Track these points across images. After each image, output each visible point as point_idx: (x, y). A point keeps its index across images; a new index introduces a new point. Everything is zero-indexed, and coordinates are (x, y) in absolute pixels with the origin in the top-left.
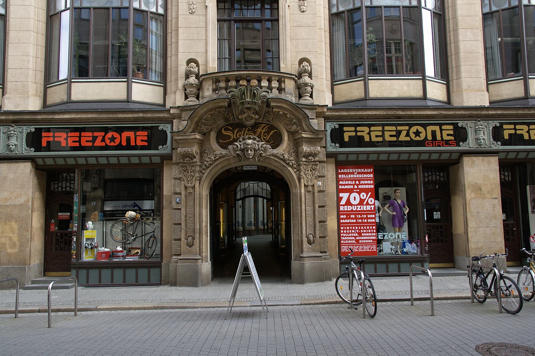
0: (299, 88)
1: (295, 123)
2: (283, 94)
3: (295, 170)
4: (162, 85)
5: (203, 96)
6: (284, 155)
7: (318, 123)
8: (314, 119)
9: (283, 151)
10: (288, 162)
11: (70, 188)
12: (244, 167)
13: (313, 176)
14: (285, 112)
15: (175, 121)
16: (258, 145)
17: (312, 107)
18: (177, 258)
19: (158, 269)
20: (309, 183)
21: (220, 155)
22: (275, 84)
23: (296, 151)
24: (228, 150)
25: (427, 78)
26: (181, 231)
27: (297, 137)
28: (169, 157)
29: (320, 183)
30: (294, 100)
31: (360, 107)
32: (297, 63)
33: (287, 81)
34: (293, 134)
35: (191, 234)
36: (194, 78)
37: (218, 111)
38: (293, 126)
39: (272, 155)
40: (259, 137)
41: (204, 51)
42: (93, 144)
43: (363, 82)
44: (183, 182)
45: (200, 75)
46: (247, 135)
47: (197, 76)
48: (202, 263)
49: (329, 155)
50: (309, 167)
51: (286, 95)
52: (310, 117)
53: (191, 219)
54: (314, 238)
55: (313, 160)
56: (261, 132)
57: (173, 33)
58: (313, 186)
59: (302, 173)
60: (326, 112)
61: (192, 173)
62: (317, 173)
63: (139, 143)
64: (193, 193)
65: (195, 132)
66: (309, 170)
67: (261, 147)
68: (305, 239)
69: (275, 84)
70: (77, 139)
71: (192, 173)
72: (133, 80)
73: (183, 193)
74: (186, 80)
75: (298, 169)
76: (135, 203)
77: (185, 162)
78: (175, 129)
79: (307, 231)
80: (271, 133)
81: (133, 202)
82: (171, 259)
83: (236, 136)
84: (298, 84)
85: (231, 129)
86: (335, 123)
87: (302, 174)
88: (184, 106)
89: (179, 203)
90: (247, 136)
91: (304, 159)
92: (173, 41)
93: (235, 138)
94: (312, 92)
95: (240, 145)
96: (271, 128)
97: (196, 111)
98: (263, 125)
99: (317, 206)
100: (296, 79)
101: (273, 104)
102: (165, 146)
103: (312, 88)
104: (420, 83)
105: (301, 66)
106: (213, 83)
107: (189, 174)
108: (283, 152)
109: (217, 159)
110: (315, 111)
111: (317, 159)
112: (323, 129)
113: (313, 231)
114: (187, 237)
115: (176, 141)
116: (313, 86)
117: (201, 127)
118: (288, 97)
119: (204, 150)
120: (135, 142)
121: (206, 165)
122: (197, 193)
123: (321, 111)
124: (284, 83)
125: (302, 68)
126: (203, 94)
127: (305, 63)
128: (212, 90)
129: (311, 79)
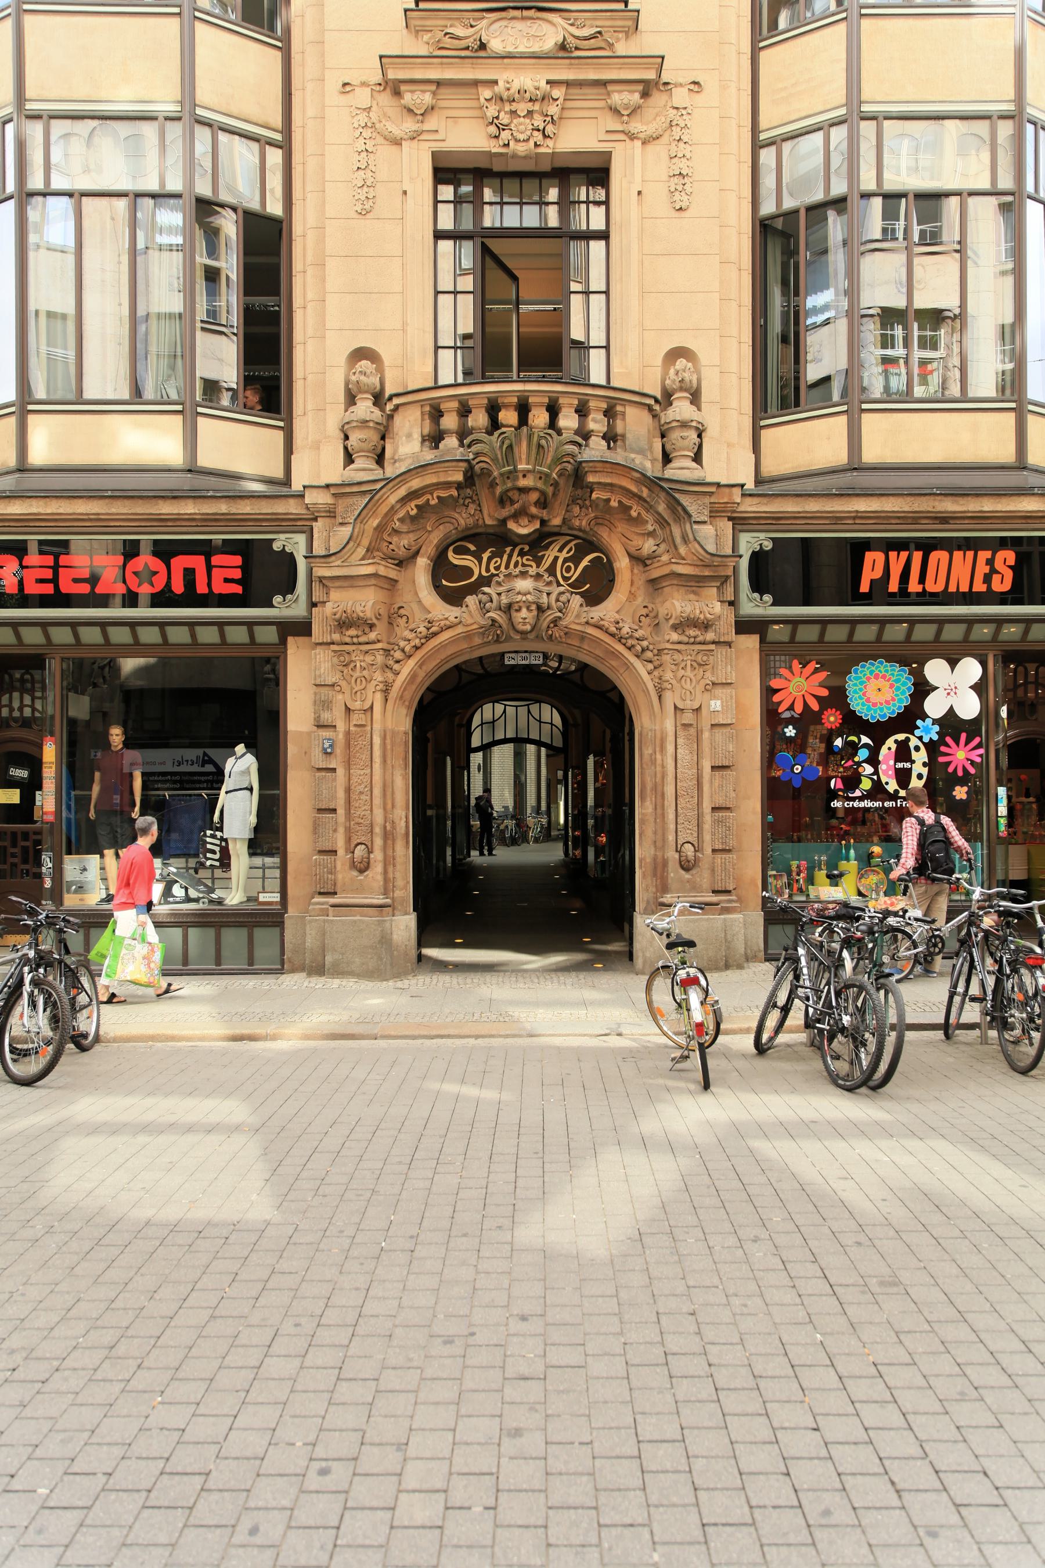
0: (663, 436)
1: (651, 534)
2: (619, 450)
3: (650, 666)
4: (281, 424)
5: (396, 457)
6: (621, 625)
8: (704, 522)
9: (617, 612)
10: (630, 642)
11: (34, 710)
12: (506, 655)
14: (627, 502)
15: (318, 526)
16: (548, 594)
17: (700, 488)
19: (277, 930)
20: (688, 702)
21: (442, 623)
22: (596, 423)
24: (464, 609)
25: (1031, 407)
26: (335, 831)
27: (655, 574)
28: (302, 628)
29: (719, 703)
30: (650, 467)
31: (834, 491)
32: (659, 361)
33: (631, 412)
34: (647, 565)
35: (362, 839)
36: (370, 403)
37: (439, 497)
39: (587, 623)
41: (399, 327)
42: (93, 587)
43: (843, 419)
44: (340, 697)
45: (387, 395)
46: (516, 565)
47: (378, 398)
49: (744, 626)
51: (626, 454)
52: (696, 517)
53: (363, 797)
56: (556, 558)
57: (310, 271)
58: (698, 710)
59: (668, 675)
61: (365, 673)
62: (708, 674)
63: (220, 588)
64: (369, 728)
65: (374, 557)
67: (557, 600)
68: (672, 855)
69: (596, 423)
70: (49, 574)
71: (365, 673)
72: (200, 410)
73: (341, 727)
74: (346, 411)
75: (657, 663)
76: (205, 754)
77: (348, 640)
78: (318, 549)
80: (585, 562)
81: (200, 752)
82: (310, 904)
83: (488, 570)
84: (662, 422)
85: (472, 548)
86: (762, 535)
87: (668, 678)
88: (342, 485)
89: (330, 753)
90: (517, 570)
91: (675, 636)
92: (310, 295)
93: (484, 574)
94: (700, 446)
95: (499, 594)
96: (587, 545)
97: (377, 497)
98: (563, 540)
100: (657, 407)
101: (591, 478)
102: (289, 596)
103: (700, 436)
104: (1010, 418)
105: (672, 371)
106: (423, 420)
107: (357, 674)
108: (617, 617)
109: (435, 634)
110: (707, 500)
112: (729, 552)
113: (696, 835)
114: (353, 846)
115: (321, 581)
116: (704, 430)
120: (209, 585)
121: (403, 650)
122: (377, 726)
123: (725, 500)
124: (624, 419)
125: (675, 377)
126: (395, 451)
127: (681, 363)
129: (699, 409)
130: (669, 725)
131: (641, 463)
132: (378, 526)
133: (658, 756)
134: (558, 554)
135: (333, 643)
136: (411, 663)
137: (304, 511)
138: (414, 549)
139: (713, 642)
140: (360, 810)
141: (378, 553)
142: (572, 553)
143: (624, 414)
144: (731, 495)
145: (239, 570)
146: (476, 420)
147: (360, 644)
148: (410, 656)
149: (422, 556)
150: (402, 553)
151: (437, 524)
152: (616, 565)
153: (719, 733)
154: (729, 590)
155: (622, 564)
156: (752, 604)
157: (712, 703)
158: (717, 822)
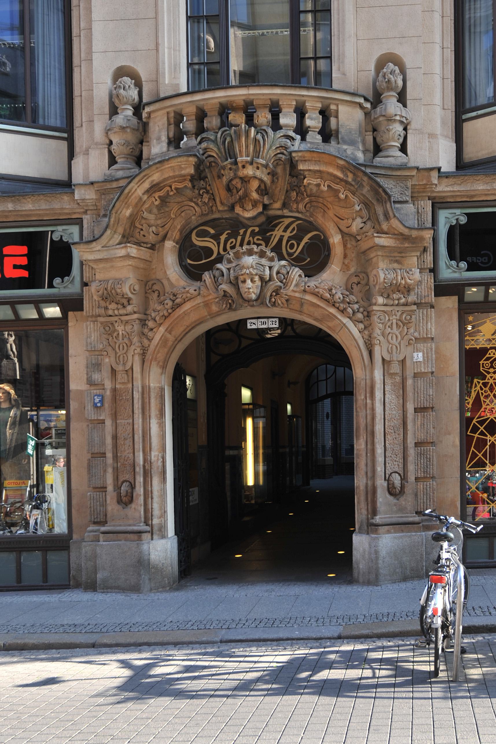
3: (361, 326)
7: (418, 212)
8: (406, 202)
13: (402, 339)
18: (98, 530)
23: (363, 282)
29: (420, 355)
38: (353, 220)
40: (277, 249)
48: (152, 539)
50: (394, 317)
51: (339, 146)
54: (403, 482)
55: (403, 301)
58: (403, 362)
60: (436, 185)
62: (412, 330)
66: (394, 326)
75: (366, 323)
77: (110, 312)
79: (387, 464)
80: (306, 240)
83: (225, 250)
85: (212, 231)
86: (458, 211)
98: (287, 221)
99: (410, 408)
111: (412, 298)
113: (401, 466)
117: (142, 230)
118: (345, 151)
119: (153, 285)
128: (167, 141)
130: (378, 374)
131: (352, 153)
132: (131, 215)
133: (369, 401)
134: (283, 234)
135: (99, 316)
136: (162, 329)
137: (76, 206)
138: (162, 232)
139: (415, 304)
140: (125, 452)
141: (131, 239)
142: (295, 232)
143: (337, 111)
144: (429, 177)
145: (26, 258)
146: (210, 122)
147: (121, 315)
148: (160, 325)
149: (169, 240)
150: (151, 238)
151: (179, 212)
152: (331, 241)
153: (420, 383)
154: (429, 258)
155: (335, 239)
156: (450, 271)
157: (415, 354)
158: (420, 455)
